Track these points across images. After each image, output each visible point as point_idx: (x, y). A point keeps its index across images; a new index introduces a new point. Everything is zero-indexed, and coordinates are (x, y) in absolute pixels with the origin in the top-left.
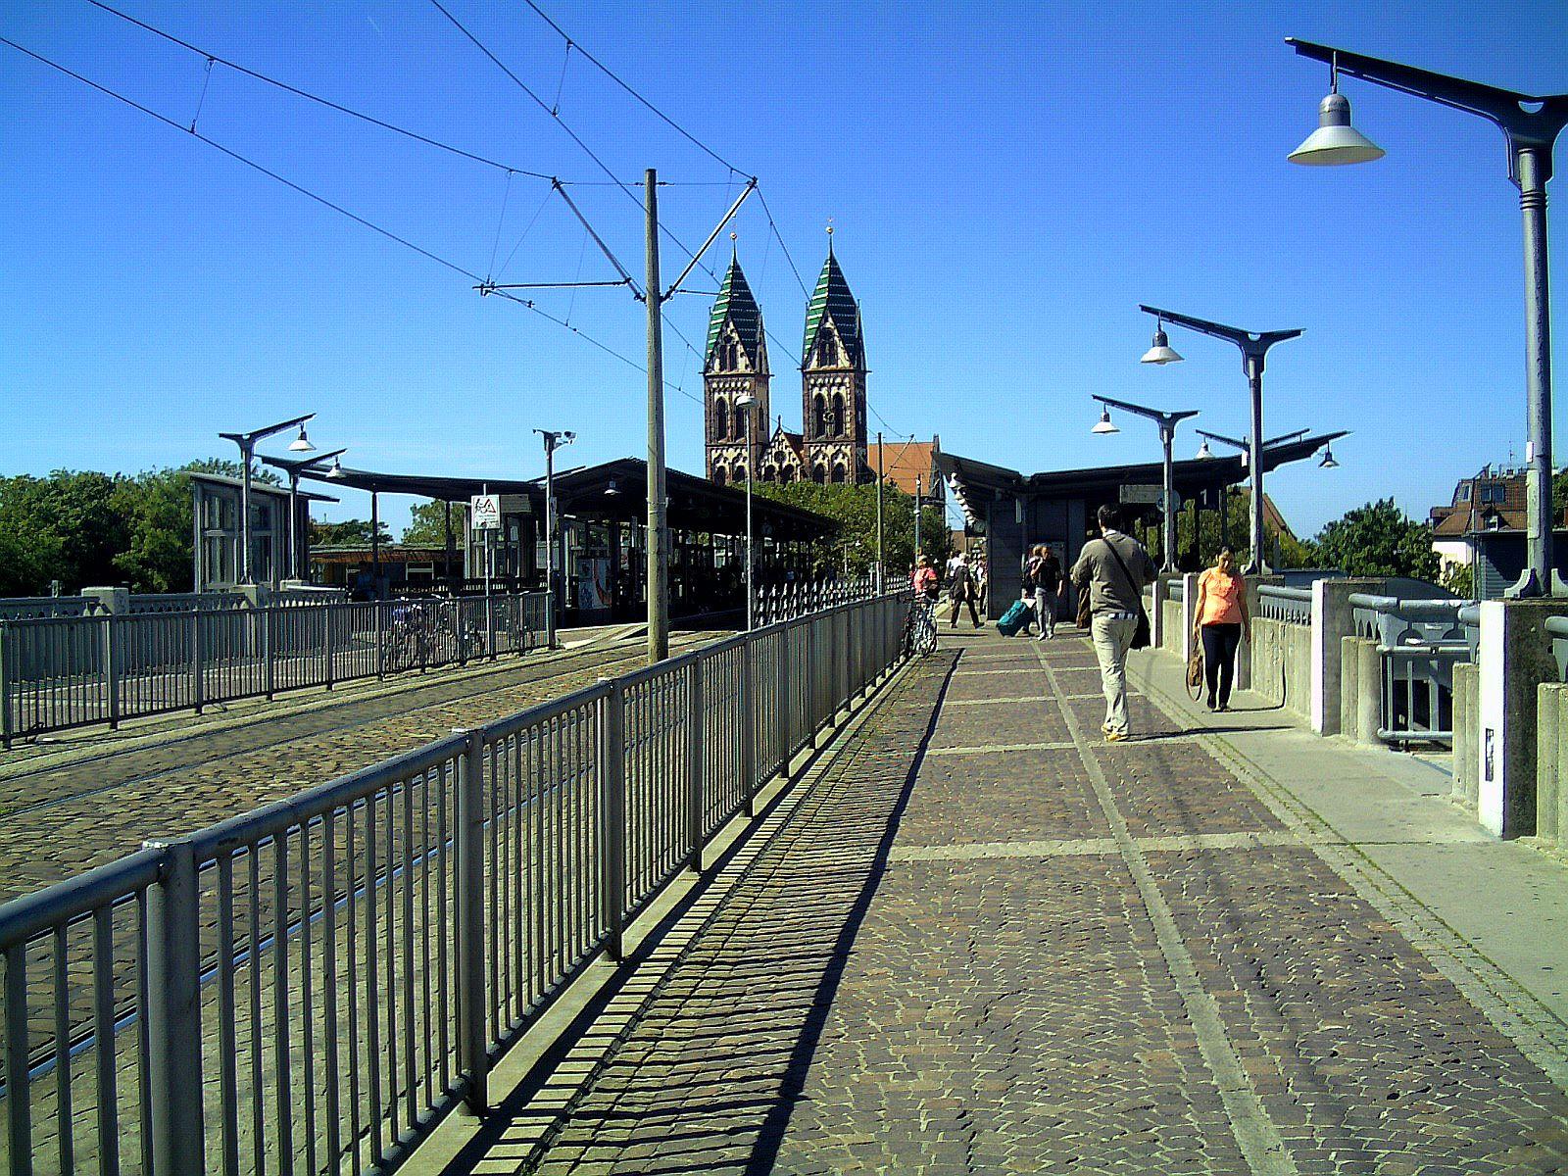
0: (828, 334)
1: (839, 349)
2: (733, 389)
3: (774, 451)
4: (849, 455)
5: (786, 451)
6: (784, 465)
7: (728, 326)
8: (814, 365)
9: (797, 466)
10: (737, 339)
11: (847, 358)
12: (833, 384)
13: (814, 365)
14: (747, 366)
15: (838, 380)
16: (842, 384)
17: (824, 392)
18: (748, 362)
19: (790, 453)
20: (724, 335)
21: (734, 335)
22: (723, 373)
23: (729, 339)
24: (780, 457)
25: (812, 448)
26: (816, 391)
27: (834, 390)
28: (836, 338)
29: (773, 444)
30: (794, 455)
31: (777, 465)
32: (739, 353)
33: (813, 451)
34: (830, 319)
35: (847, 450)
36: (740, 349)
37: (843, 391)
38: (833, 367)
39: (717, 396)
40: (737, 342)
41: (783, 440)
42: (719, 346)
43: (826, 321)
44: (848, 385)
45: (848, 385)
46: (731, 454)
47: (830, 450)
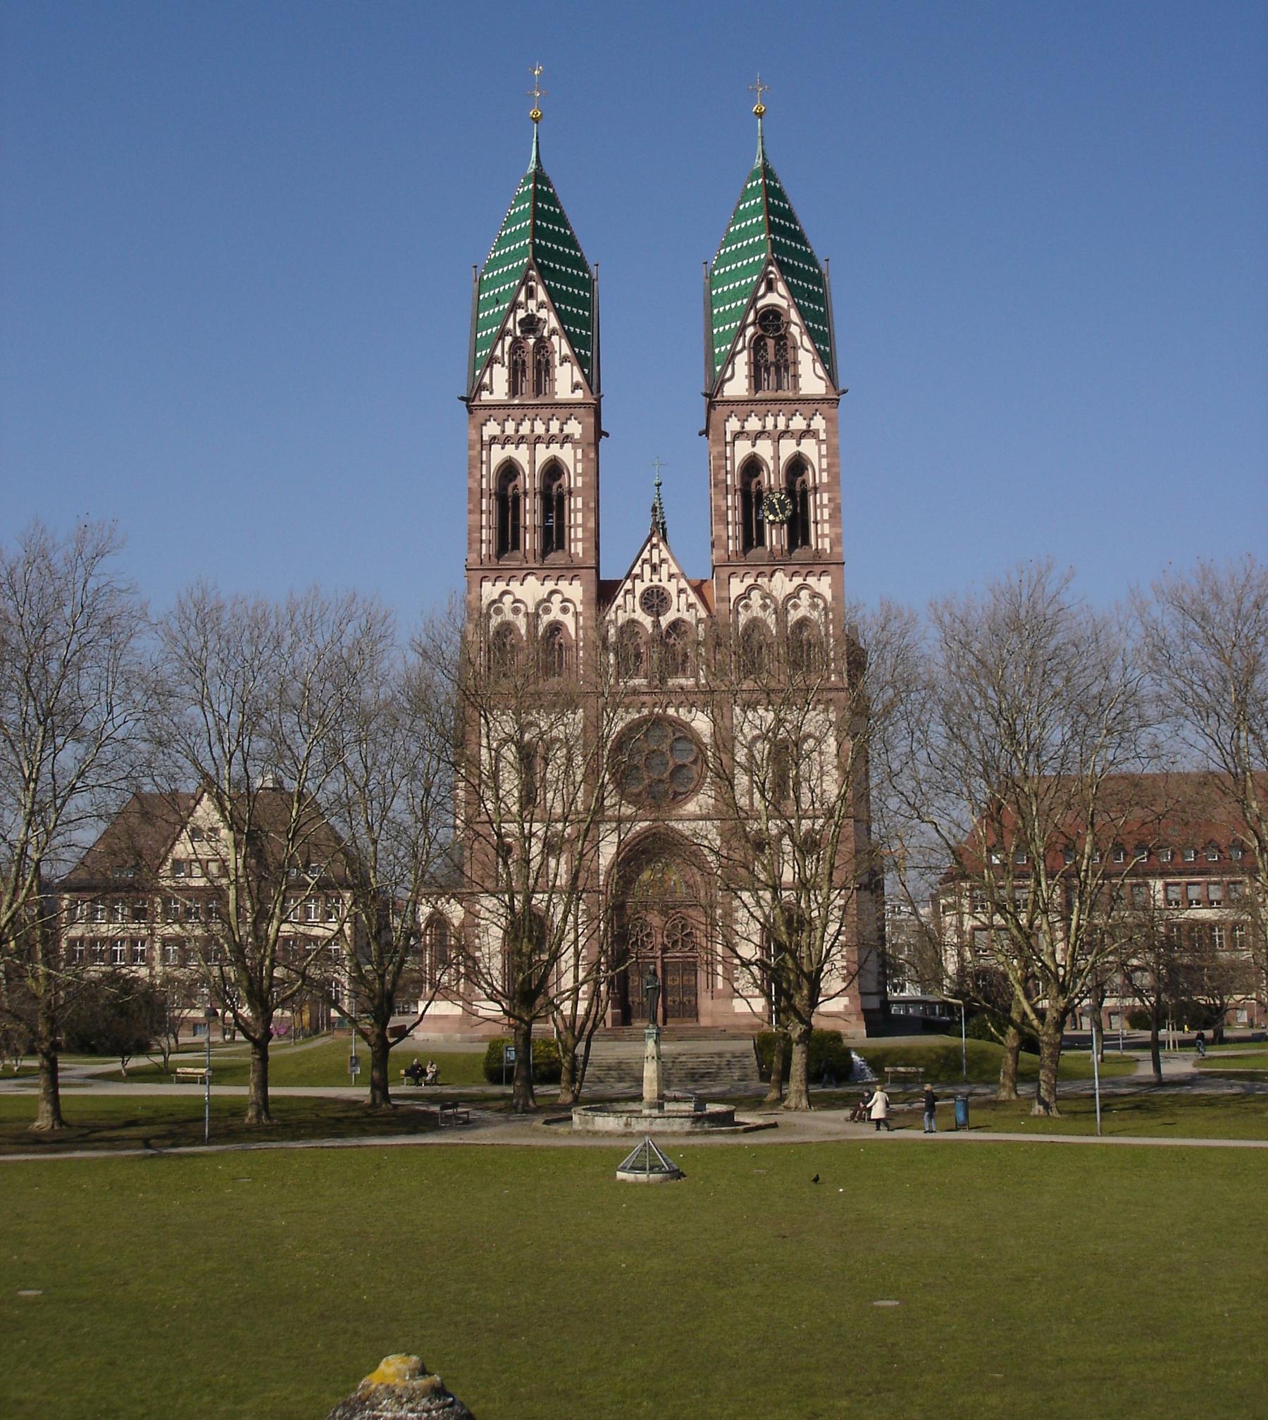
0: (771, 320)
1: (801, 352)
2: (538, 439)
3: (640, 587)
4: (829, 597)
5: (672, 587)
6: (665, 621)
7: (531, 294)
8: (737, 386)
9: (699, 621)
10: (553, 323)
11: (820, 372)
12: (785, 433)
13: (737, 386)
14: (576, 386)
15: (798, 423)
16: (808, 433)
17: (764, 449)
18: (578, 377)
19: (681, 591)
20: (521, 314)
21: (543, 314)
22: (516, 402)
23: (531, 324)
24: (655, 601)
25: (735, 582)
26: (743, 449)
27: (788, 448)
28: (794, 330)
29: (637, 570)
30: (693, 598)
31: (647, 621)
32: (557, 356)
33: (737, 587)
34: (781, 287)
35: (823, 585)
36: (560, 346)
37: (809, 448)
38: (790, 394)
39: (498, 455)
40: (553, 332)
41: (663, 561)
42: (509, 340)
43: (770, 287)
44: (823, 436)
45: (823, 436)
46: (530, 590)
47: (781, 584)
